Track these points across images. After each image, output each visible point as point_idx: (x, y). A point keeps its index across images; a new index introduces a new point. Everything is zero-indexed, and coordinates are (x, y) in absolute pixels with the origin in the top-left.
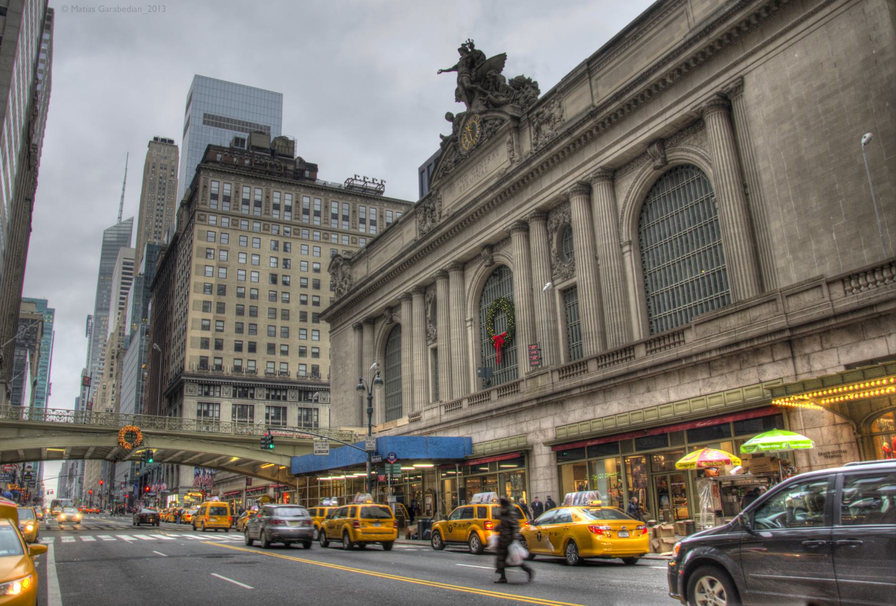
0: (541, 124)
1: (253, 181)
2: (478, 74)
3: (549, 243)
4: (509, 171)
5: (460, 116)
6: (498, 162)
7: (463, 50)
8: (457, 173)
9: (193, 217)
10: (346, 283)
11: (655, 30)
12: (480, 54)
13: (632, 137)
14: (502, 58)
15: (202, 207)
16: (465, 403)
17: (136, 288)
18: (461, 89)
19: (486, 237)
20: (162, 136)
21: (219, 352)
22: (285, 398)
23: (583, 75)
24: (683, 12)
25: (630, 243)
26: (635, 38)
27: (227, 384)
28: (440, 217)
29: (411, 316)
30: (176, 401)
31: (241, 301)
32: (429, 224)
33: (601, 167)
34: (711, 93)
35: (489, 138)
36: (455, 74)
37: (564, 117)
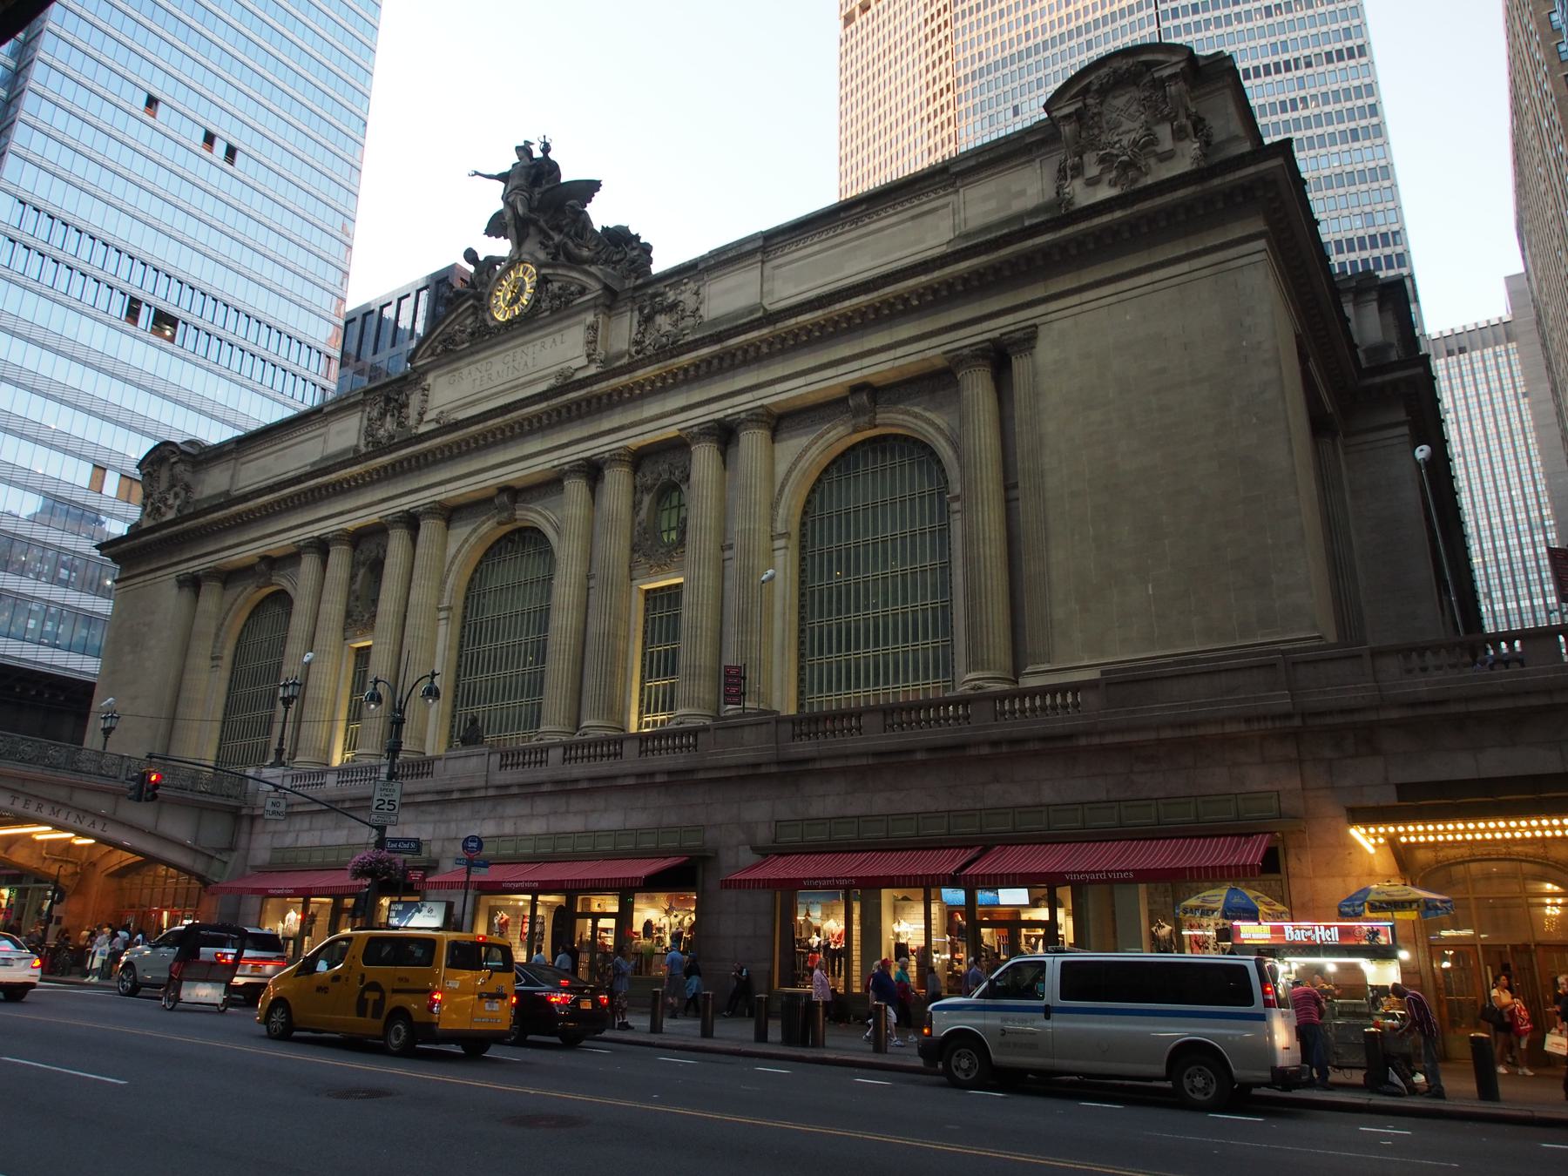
0: (654, 312)
2: (542, 200)
3: (636, 506)
4: (580, 375)
5: (492, 261)
6: (562, 350)
7: (524, 150)
8: (472, 354)
10: (176, 496)
11: (894, 219)
12: (554, 168)
14: (591, 187)
16: (555, 755)
18: (508, 215)
19: (512, 475)
24: (946, 206)
26: (856, 221)
28: (420, 421)
33: (762, 406)
34: (979, 338)
35: (553, 311)
37: (701, 312)
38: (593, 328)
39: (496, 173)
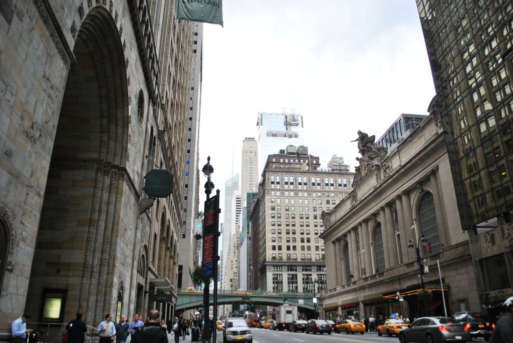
0: (386, 169)
1: (289, 174)
4: (377, 187)
5: (361, 158)
9: (264, 192)
13: (411, 181)
15: (268, 188)
17: (243, 214)
20: (248, 137)
21: (280, 251)
22: (311, 270)
23: (396, 152)
25: (415, 220)
27: (285, 265)
29: (351, 239)
30: (264, 274)
31: (288, 228)
32: (354, 202)
36: (357, 142)
38: (376, 175)
39: (355, 139)
